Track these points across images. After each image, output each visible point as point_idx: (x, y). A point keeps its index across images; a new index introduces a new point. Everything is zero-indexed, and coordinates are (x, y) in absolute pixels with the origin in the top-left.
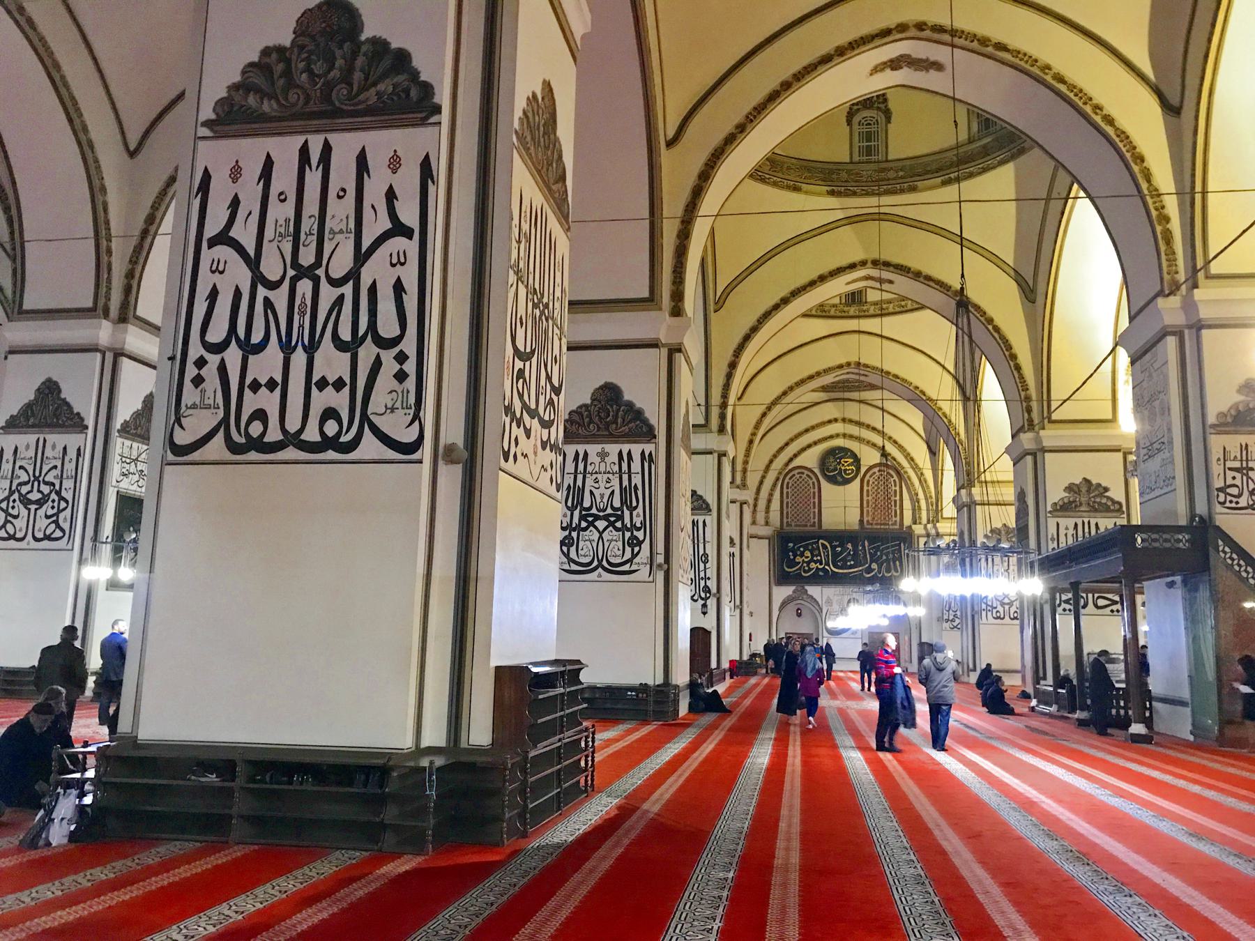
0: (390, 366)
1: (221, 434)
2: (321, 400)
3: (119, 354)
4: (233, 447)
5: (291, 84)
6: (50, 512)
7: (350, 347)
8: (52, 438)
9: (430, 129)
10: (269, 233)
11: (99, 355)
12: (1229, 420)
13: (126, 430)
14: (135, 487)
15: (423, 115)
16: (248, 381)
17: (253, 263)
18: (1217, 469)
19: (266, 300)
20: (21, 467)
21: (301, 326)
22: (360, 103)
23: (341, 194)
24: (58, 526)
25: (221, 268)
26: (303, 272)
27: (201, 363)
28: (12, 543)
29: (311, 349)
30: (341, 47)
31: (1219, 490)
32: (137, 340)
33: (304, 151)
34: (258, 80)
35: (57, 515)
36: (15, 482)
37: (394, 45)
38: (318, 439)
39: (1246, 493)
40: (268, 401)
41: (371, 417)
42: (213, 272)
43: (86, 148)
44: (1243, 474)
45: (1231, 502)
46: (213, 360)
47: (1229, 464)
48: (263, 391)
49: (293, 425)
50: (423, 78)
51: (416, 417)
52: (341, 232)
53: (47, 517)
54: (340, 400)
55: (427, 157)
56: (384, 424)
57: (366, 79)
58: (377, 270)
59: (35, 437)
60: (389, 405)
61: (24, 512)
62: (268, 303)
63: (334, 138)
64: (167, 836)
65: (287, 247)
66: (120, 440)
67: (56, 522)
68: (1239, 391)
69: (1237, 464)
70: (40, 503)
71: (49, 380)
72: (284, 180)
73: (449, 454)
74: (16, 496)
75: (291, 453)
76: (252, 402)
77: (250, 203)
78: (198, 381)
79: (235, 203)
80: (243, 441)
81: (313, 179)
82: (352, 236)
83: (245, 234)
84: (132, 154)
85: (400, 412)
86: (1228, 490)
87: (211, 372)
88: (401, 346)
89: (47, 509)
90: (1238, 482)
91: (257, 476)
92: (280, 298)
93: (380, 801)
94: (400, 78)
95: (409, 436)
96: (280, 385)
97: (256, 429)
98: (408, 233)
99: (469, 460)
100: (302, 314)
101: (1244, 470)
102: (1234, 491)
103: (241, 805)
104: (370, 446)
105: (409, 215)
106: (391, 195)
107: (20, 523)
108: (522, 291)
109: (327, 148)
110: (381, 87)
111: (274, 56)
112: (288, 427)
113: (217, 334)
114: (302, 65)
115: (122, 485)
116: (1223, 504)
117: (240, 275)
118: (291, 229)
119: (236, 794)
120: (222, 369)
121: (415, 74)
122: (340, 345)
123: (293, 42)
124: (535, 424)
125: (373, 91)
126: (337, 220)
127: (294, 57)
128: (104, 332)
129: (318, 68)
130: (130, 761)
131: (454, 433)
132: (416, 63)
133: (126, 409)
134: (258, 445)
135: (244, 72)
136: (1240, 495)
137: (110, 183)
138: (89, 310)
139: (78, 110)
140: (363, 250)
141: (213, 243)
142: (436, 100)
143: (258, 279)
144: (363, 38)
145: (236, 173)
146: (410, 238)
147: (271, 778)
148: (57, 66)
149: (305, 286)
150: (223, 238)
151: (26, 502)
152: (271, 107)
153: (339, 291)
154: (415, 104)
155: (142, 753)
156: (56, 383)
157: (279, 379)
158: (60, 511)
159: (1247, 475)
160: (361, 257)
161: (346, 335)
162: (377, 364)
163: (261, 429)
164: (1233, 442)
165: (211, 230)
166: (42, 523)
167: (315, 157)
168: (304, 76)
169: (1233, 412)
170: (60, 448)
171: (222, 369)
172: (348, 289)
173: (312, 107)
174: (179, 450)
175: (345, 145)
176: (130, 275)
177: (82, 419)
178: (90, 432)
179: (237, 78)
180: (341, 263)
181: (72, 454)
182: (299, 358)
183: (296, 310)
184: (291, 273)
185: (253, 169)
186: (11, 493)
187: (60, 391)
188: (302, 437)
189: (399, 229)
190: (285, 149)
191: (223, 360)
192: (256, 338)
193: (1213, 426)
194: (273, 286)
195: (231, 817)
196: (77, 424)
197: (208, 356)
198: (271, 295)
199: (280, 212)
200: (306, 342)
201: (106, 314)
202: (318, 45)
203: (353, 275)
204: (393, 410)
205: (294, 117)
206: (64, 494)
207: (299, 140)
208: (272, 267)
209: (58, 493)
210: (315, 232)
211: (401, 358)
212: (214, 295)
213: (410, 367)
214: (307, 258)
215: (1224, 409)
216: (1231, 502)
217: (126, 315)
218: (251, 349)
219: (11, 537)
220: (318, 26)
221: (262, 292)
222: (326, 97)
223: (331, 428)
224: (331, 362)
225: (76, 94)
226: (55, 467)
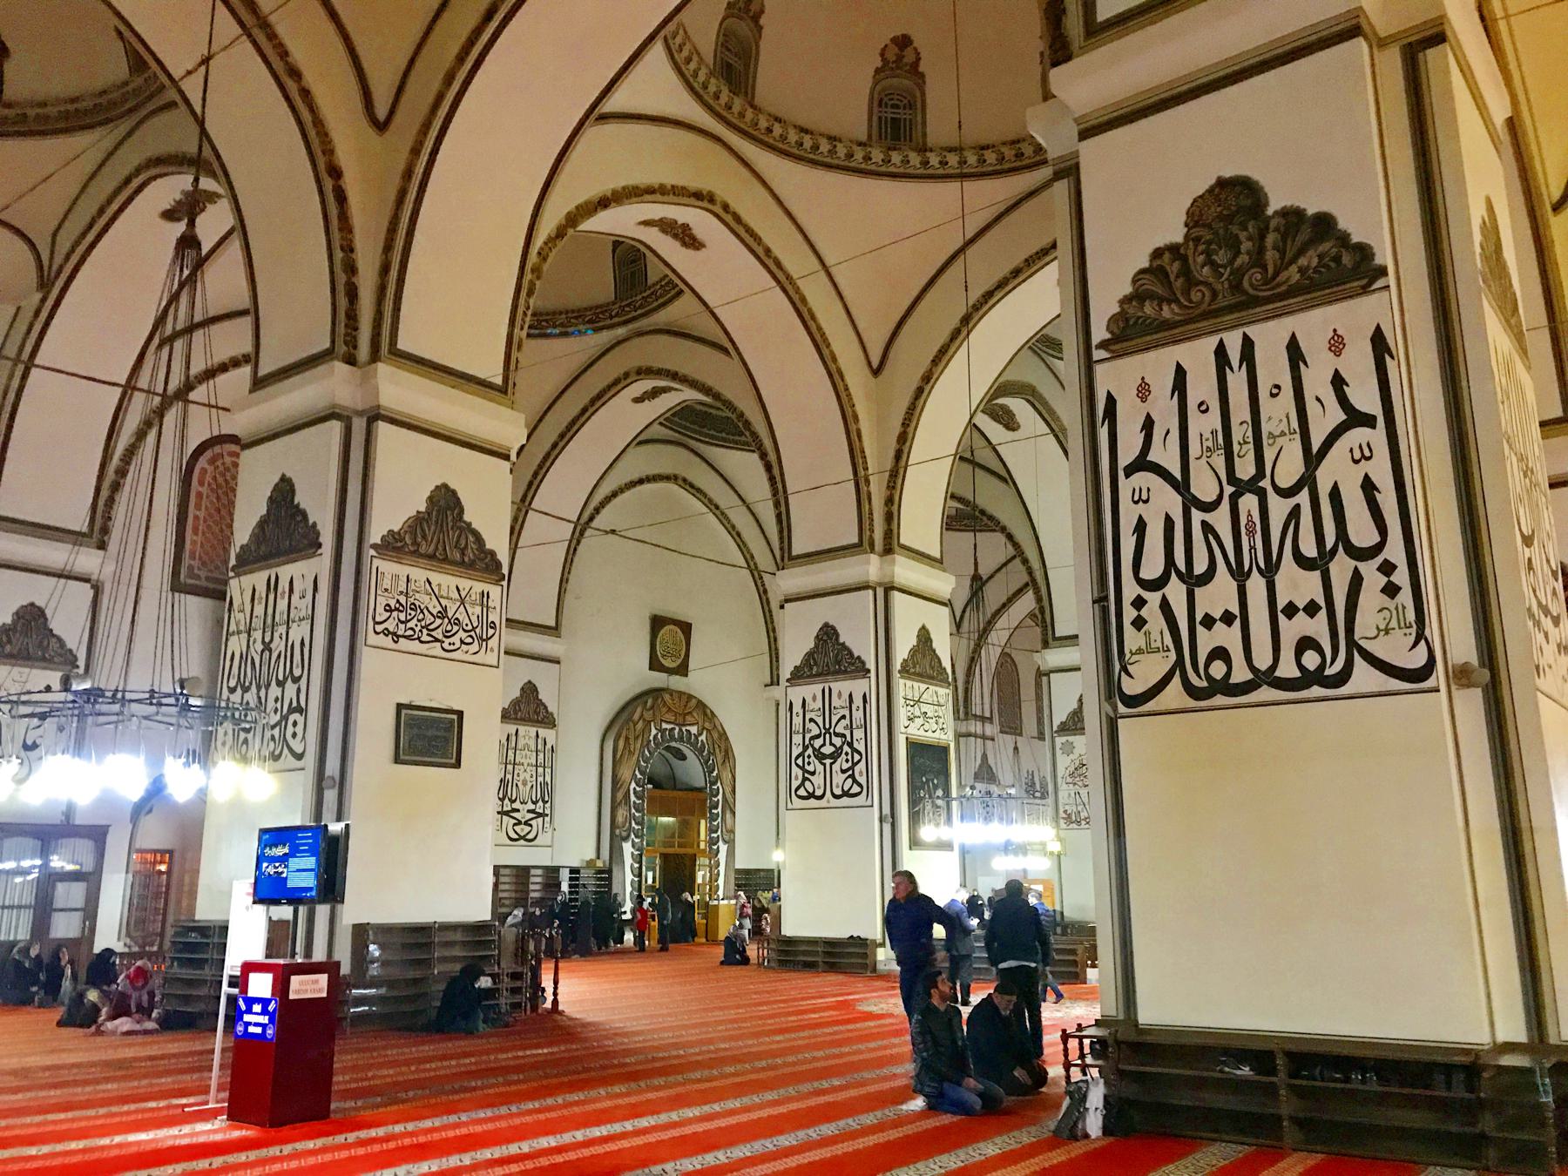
0: (1373, 579)
1: (1177, 679)
2: (1291, 630)
3: (889, 588)
5: (1191, 282)
6: (845, 766)
7: (1318, 564)
8: (837, 686)
9: (1376, 296)
10: (1194, 449)
11: (871, 592)
13: (905, 671)
14: (921, 732)
15: (1364, 282)
16: (1199, 617)
17: (1181, 486)
19: (1204, 524)
20: (811, 720)
21: (1252, 548)
22: (1279, 285)
23: (1275, 391)
24: (855, 781)
25: (1144, 497)
26: (1241, 487)
27: (1139, 603)
28: (812, 802)
30: (1246, 229)
32: (905, 571)
33: (1221, 352)
35: (852, 768)
36: (808, 736)
37: (1311, 211)
38: (1297, 674)
40: (1229, 637)
41: (1362, 643)
42: (1136, 503)
43: (836, 377)
46: (1153, 598)
48: (1219, 626)
49: (1263, 660)
50: (1355, 239)
51: (1420, 636)
52: (1283, 434)
53: (843, 772)
54: (1317, 627)
55: (1378, 328)
56: (1378, 649)
57: (1282, 258)
58: (1337, 470)
59: (821, 686)
60: (1382, 627)
61: (820, 768)
62: (1207, 528)
63: (1252, 331)
64: (1204, 1135)
65: (1219, 461)
66: (902, 681)
67: (852, 776)
70: (835, 756)
71: (826, 625)
72: (1202, 387)
73: (1462, 676)
74: (810, 751)
75: (1266, 693)
76: (1207, 641)
77: (1166, 418)
78: (1139, 623)
79: (1148, 425)
80: (1205, 684)
81: (1237, 381)
82: (1297, 436)
83: (1166, 454)
84: (876, 372)
85: (1398, 633)
87: (1152, 611)
88: (1386, 554)
89: (841, 763)
91: (1224, 722)
92: (1221, 520)
93: (1472, 1110)
94: (1325, 246)
95: (1418, 659)
96: (1240, 617)
97: (1218, 669)
98: (1369, 421)
99: (1491, 677)
100: (1251, 533)
103: (1287, 1106)
104: (1364, 677)
105: (1365, 398)
106: (1338, 382)
107: (818, 780)
108: (1514, 459)
109: (1248, 345)
110: (1303, 261)
111: (1167, 256)
112: (1256, 664)
113: (1153, 568)
114: (1201, 259)
115: (909, 730)
117: (1171, 501)
118: (1221, 440)
119: (1282, 1092)
120: (1165, 605)
121: (1344, 238)
122: (1302, 561)
123: (1186, 237)
124: (1547, 623)
125: (1294, 269)
126: (1275, 422)
127: (1190, 253)
128: (871, 567)
129: (1221, 257)
130: (1126, 1047)
131: (1462, 646)
132: (1342, 224)
133: (903, 646)
134: (1225, 687)
135: (1134, 281)
137: (860, 409)
138: (854, 546)
139: (825, 340)
140: (1315, 449)
141: (1130, 471)
142: (1378, 261)
143: (1191, 502)
144: (1270, 211)
145: (1144, 391)
146: (1374, 427)
147: (1321, 1073)
148: (804, 300)
149: (1249, 503)
150: (1142, 464)
151: (821, 757)
152: (1172, 311)
153: (1292, 501)
154: (1355, 270)
155: (1142, 1039)
156: (833, 628)
157: (1236, 610)
158: (855, 764)
160: (1313, 460)
161: (1309, 549)
162: (1357, 580)
163: (1224, 669)
165: (1126, 457)
166: (839, 778)
167: (1234, 355)
168: (1206, 269)
170: (846, 696)
171: (1165, 605)
172: (1303, 498)
173: (1222, 302)
174: (1133, 701)
175: (1270, 337)
176: (889, 501)
177: (863, 663)
178: (873, 674)
179: (1128, 289)
180: (1289, 468)
181: (858, 701)
182: (1256, 585)
183: (1243, 531)
184: (1229, 490)
185: (1163, 383)
186: (805, 748)
187: (838, 635)
188: (1277, 674)
189: (1356, 419)
190: (1197, 355)
191: (1164, 598)
192: (1200, 567)
195: (1279, 1119)
196: (860, 669)
197: (1146, 595)
198: (1208, 517)
199: (1204, 425)
200: (1262, 565)
201: (872, 550)
202: (1216, 233)
203: (1307, 480)
204: (1387, 631)
205: (1206, 316)
206: (856, 745)
207: (1211, 342)
208: (1204, 486)
209: (850, 745)
210: (1251, 440)
211: (1387, 568)
213: (1401, 577)
214: (1245, 469)
217: (890, 547)
218: (1194, 582)
219: (811, 795)
220: (1215, 210)
221: (1197, 516)
222: (1236, 287)
223: (1311, 660)
224: (1298, 585)
225: (824, 325)
226: (843, 717)
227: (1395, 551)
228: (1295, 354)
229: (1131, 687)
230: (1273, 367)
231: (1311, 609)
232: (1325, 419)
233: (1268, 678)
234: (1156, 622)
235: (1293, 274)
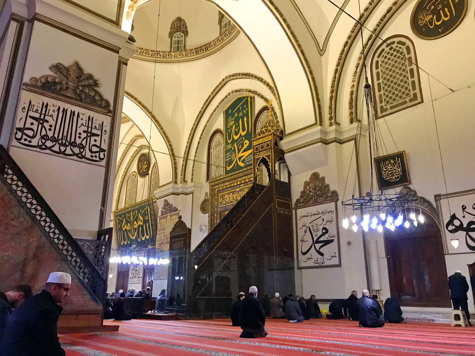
12: (39, 84)
18: (21, 114)
31: (19, 129)
39: (38, 136)
44: (39, 123)
45: (25, 140)
47: (31, 113)
68: (50, 68)
69: (37, 115)
86: (26, 132)
90: (35, 127)
101: (41, 121)
102: (30, 133)
116: (18, 140)
136: (34, 137)
159: (42, 124)
164: (38, 100)
169: (43, 80)
193: (26, 85)
215: (38, 77)
216: (25, 140)
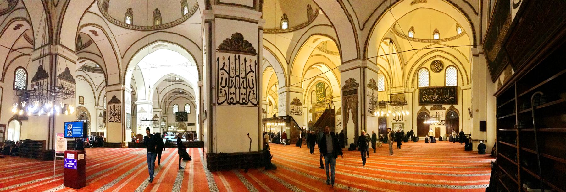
0: (252, 92)
2: (242, 96)
4: (228, 103)
7: (246, 88)
17: (229, 74)
26: (237, 76)
27: (221, 89)
29: (240, 88)
33: (235, 56)
34: (226, 43)
40: (234, 96)
49: (238, 100)
54: (245, 97)
58: (249, 77)
72: (232, 60)
75: (238, 105)
76: (231, 96)
78: (221, 92)
79: (224, 63)
87: (223, 91)
89: (117, 116)
92: (234, 80)
97: (232, 101)
104: (250, 104)
106: (250, 66)
113: (224, 84)
117: (227, 76)
120: (225, 90)
122: (244, 88)
141: (221, 69)
143: (230, 76)
150: (222, 69)
160: (246, 75)
161: (245, 87)
165: (220, 67)
166: (116, 118)
174: (219, 104)
175: (243, 57)
182: (238, 90)
185: (227, 58)
189: (252, 71)
190: (232, 56)
192: (230, 86)
194: (232, 78)
199: (232, 66)
203: (245, 77)
211: (254, 91)
212: (222, 78)
213: (255, 92)
214: (238, 74)
218: (230, 88)
221: (230, 78)
222: (238, 48)
223: (244, 101)
227: (255, 89)
228: (245, 60)
229: (219, 102)
230: (242, 61)
231: (244, 94)
232: (248, 70)
233: (238, 102)
234: (224, 93)
235: (246, 50)
